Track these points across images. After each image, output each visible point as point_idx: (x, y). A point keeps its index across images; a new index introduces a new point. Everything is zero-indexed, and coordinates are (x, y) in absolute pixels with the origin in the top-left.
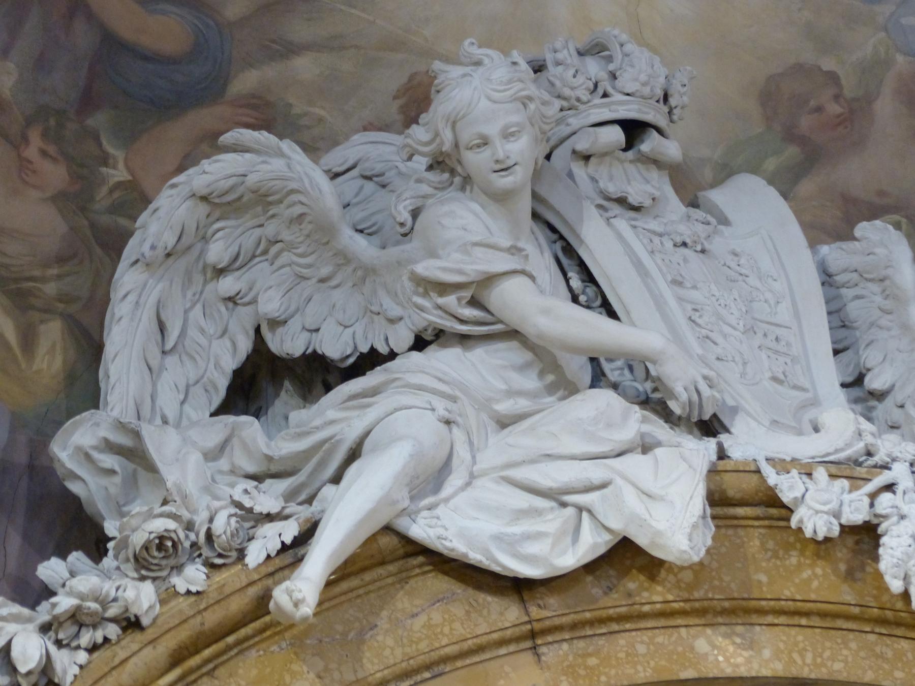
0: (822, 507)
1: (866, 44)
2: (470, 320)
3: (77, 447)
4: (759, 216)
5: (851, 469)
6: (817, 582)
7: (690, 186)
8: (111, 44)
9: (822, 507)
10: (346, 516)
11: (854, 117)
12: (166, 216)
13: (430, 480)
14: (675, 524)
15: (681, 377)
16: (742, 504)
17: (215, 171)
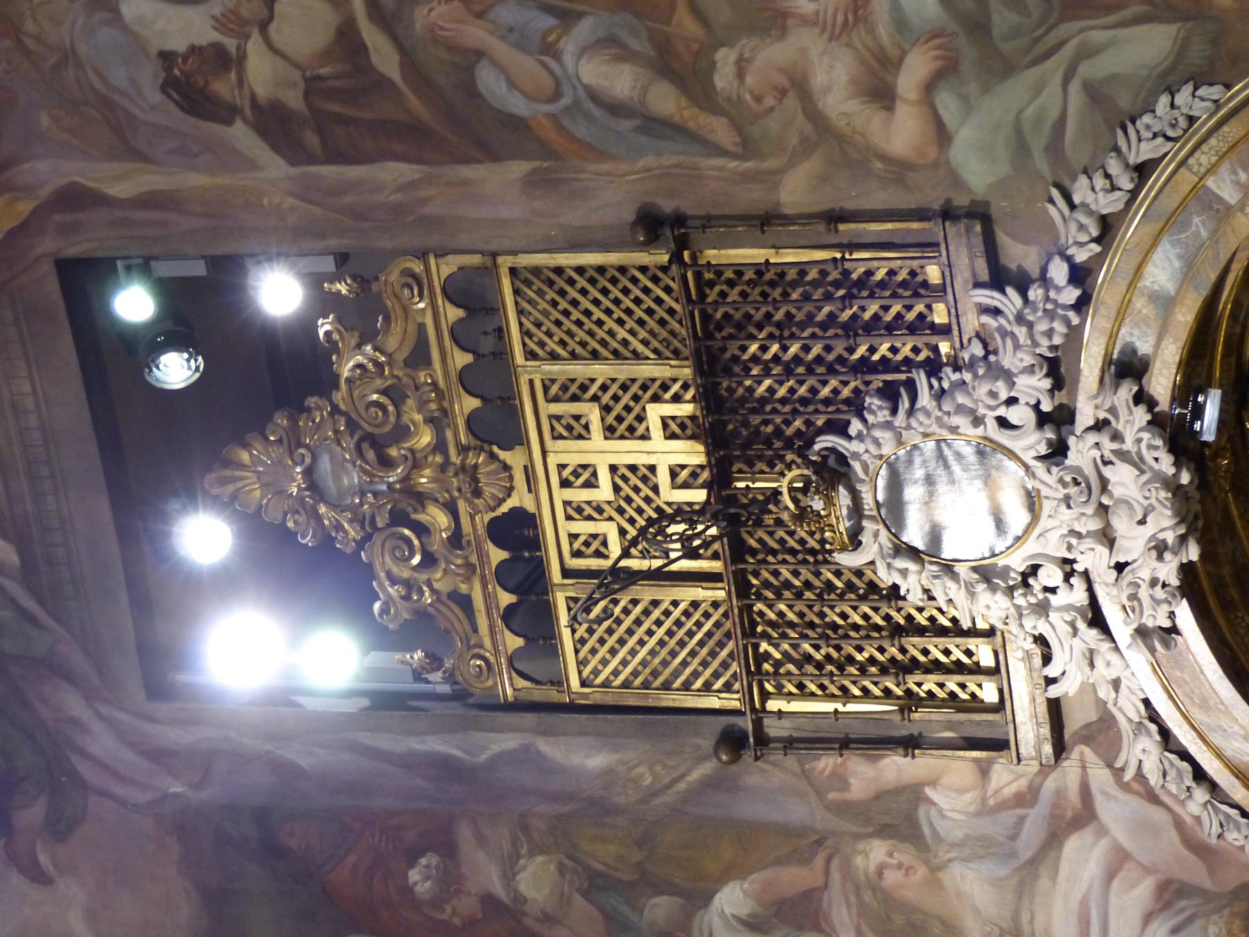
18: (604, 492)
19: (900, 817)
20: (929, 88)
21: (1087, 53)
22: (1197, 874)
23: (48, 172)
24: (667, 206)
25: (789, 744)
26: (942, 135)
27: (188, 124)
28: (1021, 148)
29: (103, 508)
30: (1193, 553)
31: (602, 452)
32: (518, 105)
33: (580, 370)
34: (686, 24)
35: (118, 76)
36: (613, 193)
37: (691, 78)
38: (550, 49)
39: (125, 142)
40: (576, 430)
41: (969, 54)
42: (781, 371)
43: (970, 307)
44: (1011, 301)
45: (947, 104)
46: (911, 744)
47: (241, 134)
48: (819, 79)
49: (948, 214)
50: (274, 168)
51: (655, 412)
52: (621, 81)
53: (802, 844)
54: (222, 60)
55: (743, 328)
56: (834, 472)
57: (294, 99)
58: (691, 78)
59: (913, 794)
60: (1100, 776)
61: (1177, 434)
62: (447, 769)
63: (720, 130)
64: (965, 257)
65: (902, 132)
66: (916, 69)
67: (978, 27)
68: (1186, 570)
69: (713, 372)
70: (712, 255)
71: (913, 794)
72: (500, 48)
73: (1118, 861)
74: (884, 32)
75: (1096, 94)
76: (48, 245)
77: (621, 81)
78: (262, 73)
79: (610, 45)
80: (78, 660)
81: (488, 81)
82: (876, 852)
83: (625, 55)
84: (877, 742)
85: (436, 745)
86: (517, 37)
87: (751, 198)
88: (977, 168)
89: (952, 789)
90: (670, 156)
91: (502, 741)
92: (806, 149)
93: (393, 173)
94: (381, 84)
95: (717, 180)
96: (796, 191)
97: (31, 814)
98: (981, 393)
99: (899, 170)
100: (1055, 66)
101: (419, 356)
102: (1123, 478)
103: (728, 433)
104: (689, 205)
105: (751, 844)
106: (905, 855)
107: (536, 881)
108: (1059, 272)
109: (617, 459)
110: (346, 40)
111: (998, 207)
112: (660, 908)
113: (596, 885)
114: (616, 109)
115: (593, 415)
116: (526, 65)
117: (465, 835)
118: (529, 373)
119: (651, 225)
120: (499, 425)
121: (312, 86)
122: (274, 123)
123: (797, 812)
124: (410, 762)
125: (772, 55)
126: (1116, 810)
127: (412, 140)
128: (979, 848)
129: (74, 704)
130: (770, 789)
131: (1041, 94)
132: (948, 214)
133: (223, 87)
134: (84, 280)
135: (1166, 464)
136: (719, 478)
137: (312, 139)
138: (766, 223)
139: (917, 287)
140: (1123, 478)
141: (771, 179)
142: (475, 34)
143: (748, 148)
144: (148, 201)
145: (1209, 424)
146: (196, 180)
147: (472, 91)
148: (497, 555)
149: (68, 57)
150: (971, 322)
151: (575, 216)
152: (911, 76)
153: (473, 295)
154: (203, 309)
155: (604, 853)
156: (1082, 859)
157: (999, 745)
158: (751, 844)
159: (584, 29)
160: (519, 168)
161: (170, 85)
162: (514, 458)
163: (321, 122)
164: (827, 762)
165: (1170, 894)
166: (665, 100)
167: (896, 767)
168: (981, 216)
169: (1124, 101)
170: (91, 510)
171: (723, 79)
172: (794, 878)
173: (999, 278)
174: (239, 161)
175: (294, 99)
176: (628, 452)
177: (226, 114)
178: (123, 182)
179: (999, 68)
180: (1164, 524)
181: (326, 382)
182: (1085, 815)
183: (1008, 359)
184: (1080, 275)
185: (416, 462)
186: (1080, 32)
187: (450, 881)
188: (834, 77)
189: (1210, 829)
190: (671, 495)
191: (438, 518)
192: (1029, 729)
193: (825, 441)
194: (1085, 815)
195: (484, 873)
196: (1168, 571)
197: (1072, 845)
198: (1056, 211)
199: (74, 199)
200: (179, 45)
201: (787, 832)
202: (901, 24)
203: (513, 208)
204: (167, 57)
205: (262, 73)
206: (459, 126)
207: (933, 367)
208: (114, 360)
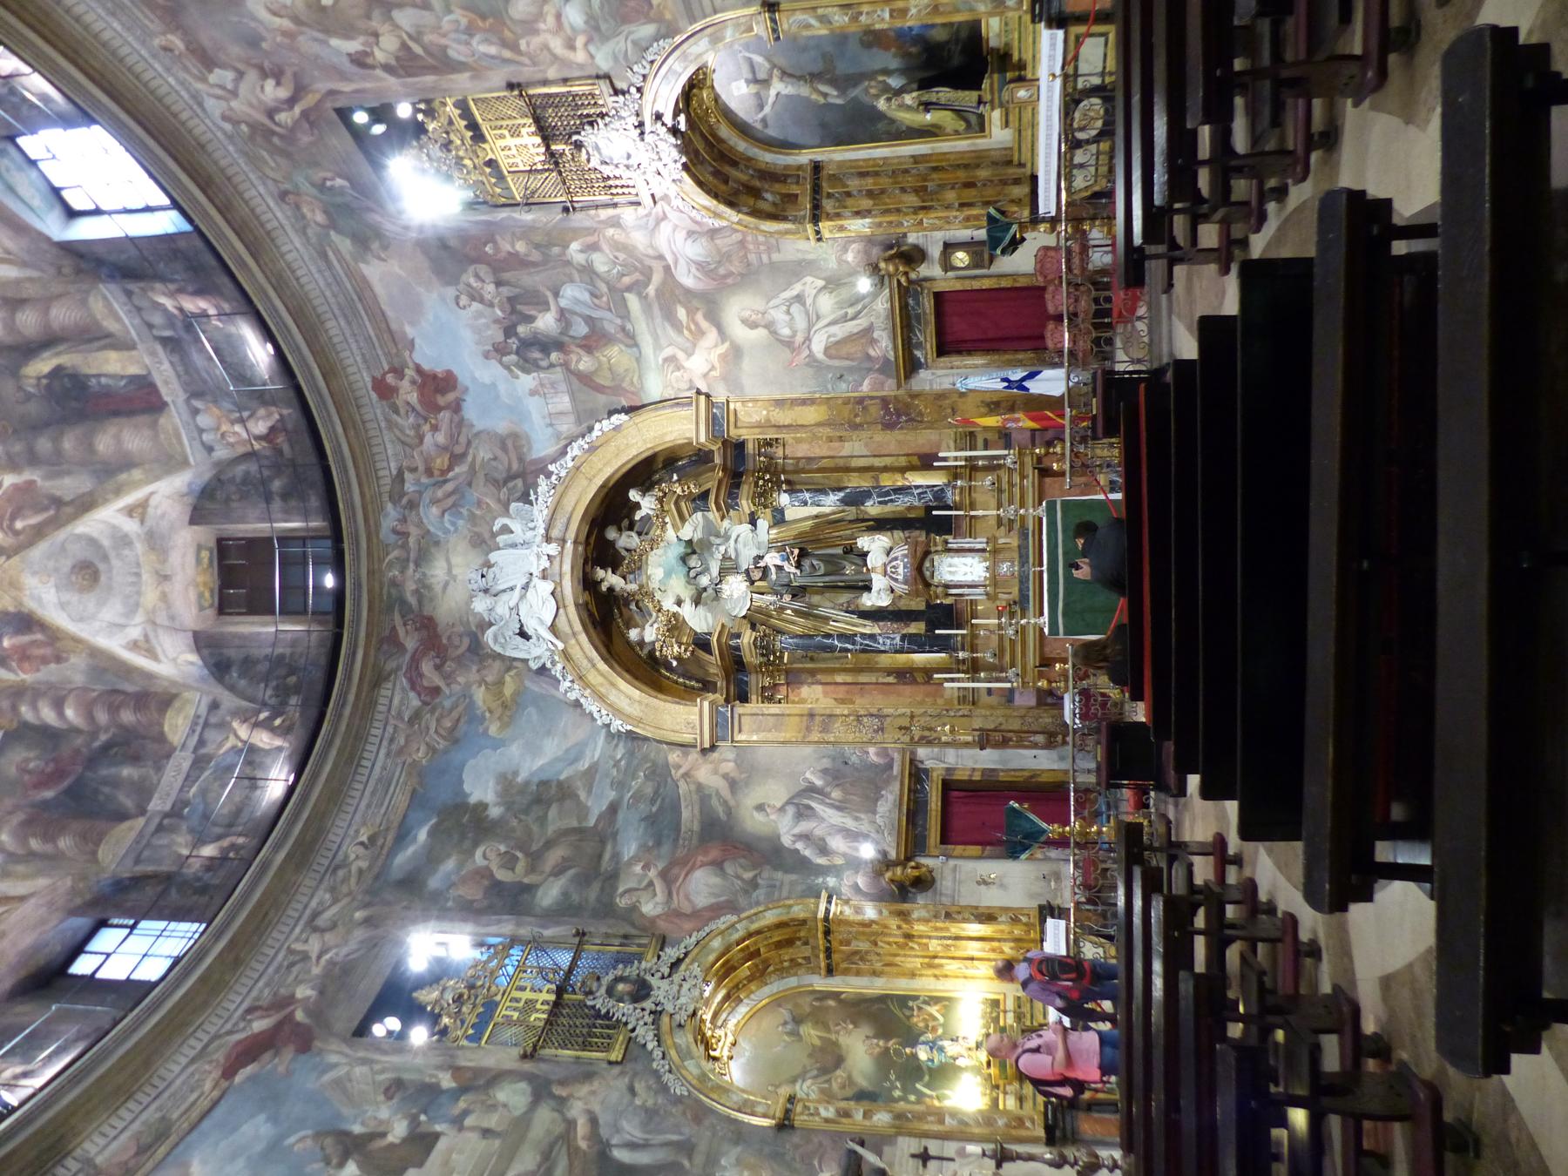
0: (545, 563)
1: (466, 532)
2: (515, 609)
3: (534, 666)
4: (494, 557)
5: (539, 557)
6: (557, 562)
7: (490, 566)
8: (469, 649)
9: (545, 563)
10: (549, 636)
11: (478, 535)
12: (498, 649)
13: (541, 622)
14: (548, 586)
15: (525, 581)
16: (544, 578)
17: (491, 643)
18: (514, 151)
19: (615, 223)
20: (586, 45)
21: (630, 33)
22: (697, 228)
23: (323, 86)
24: (514, 80)
25: (582, 209)
26: (592, 57)
27: (361, 71)
28: (616, 59)
29: (370, 169)
30: (684, 159)
31: (509, 141)
32: (462, 59)
33: (500, 123)
34: (507, 34)
35: (335, 60)
36: (499, 77)
37: (514, 47)
38: (468, 43)
39: (343, 76)
40: (502, 137)
41: (596, 38)
42: (559, 122)
43: (609, 101)
44: (621, 98)
45: (592, 49)
46: (615, 205)
47: (379, 72)
48: (552, 45)
49: (598, 77)
50: (391, 81)
51: (524, 131)
52: (493, 50)
53: (591, 231)
54: (366, 54)
55: (544, 108)
56: (579, 146)
57: (393, 62)
58: (514, 47)
59: (618, 217)
60: (667, 208)
61: (674, 131)
62: (488, 223)
63: (526, 60)
64: (603, 88)
65: (580, 56)
66: (580, 41)
67: (597, 29)
68: (684, 165)
69: (537, 120)
70: (531, 92)
71: (618, 217)
72: (455, 45)
73: (676, 227)
74: (569, 32)
75: (635, 43)
76: (329, 105)
77: (493, 50)
78: (380, 56)
79: (487, 41)
80: (373, 206)
81: (451, 53)
82: (610, 232)
83: (491, 43)
84: (606, 206)
85: (483, 218)
86: (459, 42)
87: (539, 76)
88: (603, 63)
89: (628, 215)
90: (512, 68)
91: (503, 214)
92: (552, 63)
93: (429, 79)
94: (416, 57)
95: (525, 73)
96: (552, 73)
97: (375, 246)
98: (617, 124)
99: (581, 66)
100: (622, 38)
101: (451, 122)
102: (662, 145)
103: (546, 134)
104: (521, 79)
105: (576, 233)
106: (619, 231)
107: (520, 247)
108: (633, 90)
109: (519, 147)
110: (404, 46)
111: (612, 74)
112: (556, 250)
113: (537, 246)
114: (493, 57)
115: (506, 132)
116: (462, 48)
117: (498, 238)
118: (484, 127)
119: (511, 86)
120: (479, 137)
121: (398, 59)
122: (387, 68)
123: (587, 223)
124: (477, 223)
125: (536, 41)
126: (672, 215)
127: (433, 70)
128: (640, 227)
129: (378, 218)
130: (577, 219)
131: (620, 44)
132: (598, 77)
133: (369, 61)
134: (344, 114)
135: (672, 140)
136: (548, 148)
137: (401, 72)
138: (545, 83)
139: (593, 96)
140: (662, 145)
141: (544, 72)
142: (443, 41)
143: (535, 64)
144: (357, 91)
145: (683, 127)
146: (368, 85)
147: (447, 56)
148: (488, 170)
149: (317, 57)
150: (611, 105)
151: (487, 85)
152: (580, 41)
153: (462, 105)
154: (381, 113)
155: (538, 239)
156: (665, 228)
157: (639, 204)
158: (576, 233)
159: (477, 38)
160: (467, 75)
161: (352, 61)
162: (485, 146)
163: (402, 67)
164: (592, 212)
165: (690, 233)
166: (507, 54)
167: (611, 212)
168: (607, 77)
169: (644, 44)
170: (365, 168)
171: (523, 44)
172: (590, 239)
173: (616, 92)
174: (379, 79)
175: (393, 62)
176: (518, 141)
177: (373, 67)
178: (347, 87)
179: (605, 39)
180: (675, 154)
181: (425, 131)
182: (665, 217)
183: (623, 113)
184: (639, 90)
185: (457, 149)
186: (626, 28)
187: (497, 248)
188: (557, 45)
189: (698, 218)
190: (533, 151)
191: (467, 162)
192: (647, 201)
193: (575, 138)
194: (665, 217)
195: (506, 247)
196: (679, 166)
197: (663, 224)
198: (629, 73)
199: (331, 93)
200: (352, 51)
201: (587, 229)
202: (572, 28)
203: (468, 85)
204: (349, 55)
205: (380, 56)
206: (444, 64)
207: (602, 115)
208: (359, 134)
